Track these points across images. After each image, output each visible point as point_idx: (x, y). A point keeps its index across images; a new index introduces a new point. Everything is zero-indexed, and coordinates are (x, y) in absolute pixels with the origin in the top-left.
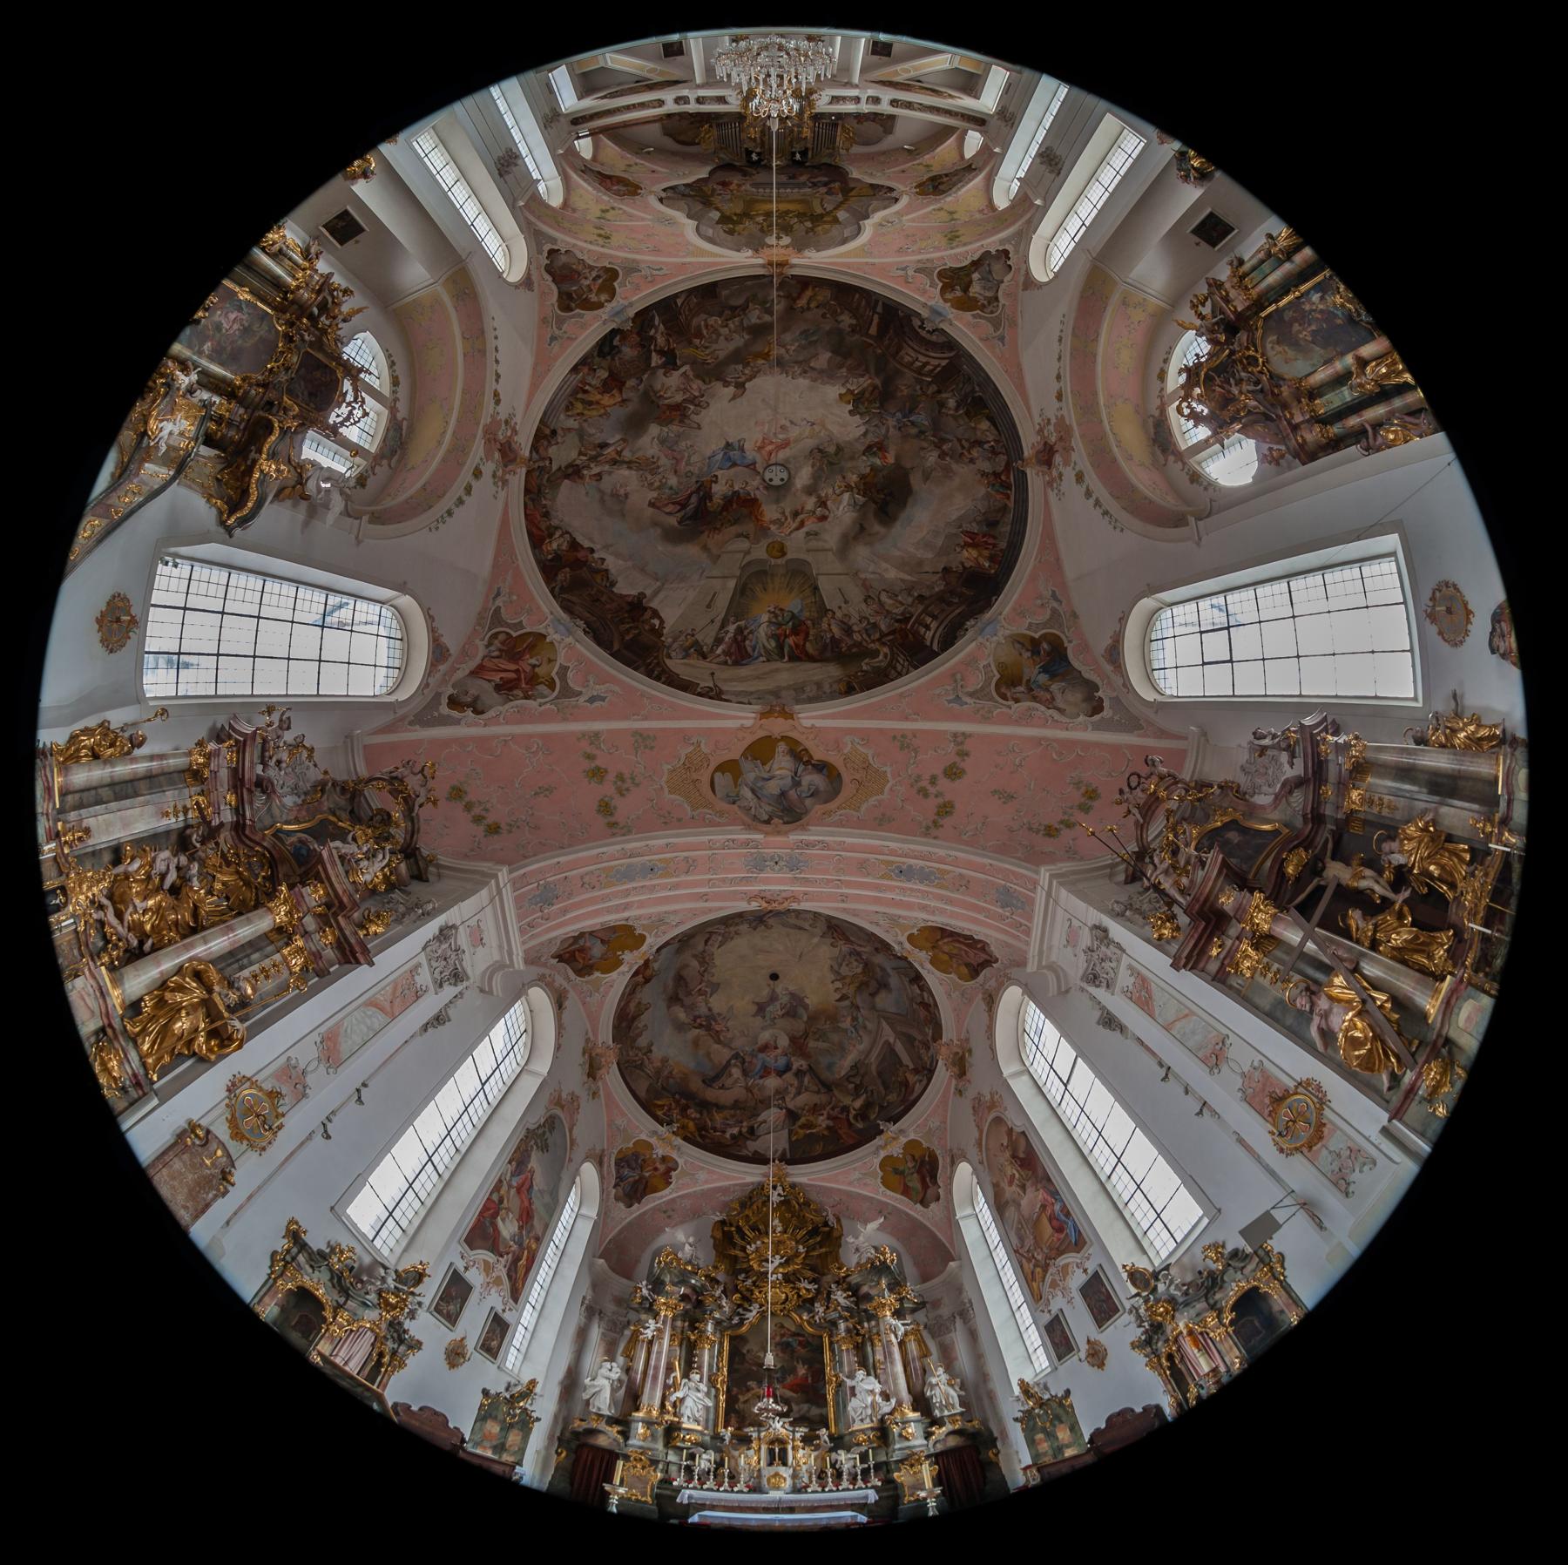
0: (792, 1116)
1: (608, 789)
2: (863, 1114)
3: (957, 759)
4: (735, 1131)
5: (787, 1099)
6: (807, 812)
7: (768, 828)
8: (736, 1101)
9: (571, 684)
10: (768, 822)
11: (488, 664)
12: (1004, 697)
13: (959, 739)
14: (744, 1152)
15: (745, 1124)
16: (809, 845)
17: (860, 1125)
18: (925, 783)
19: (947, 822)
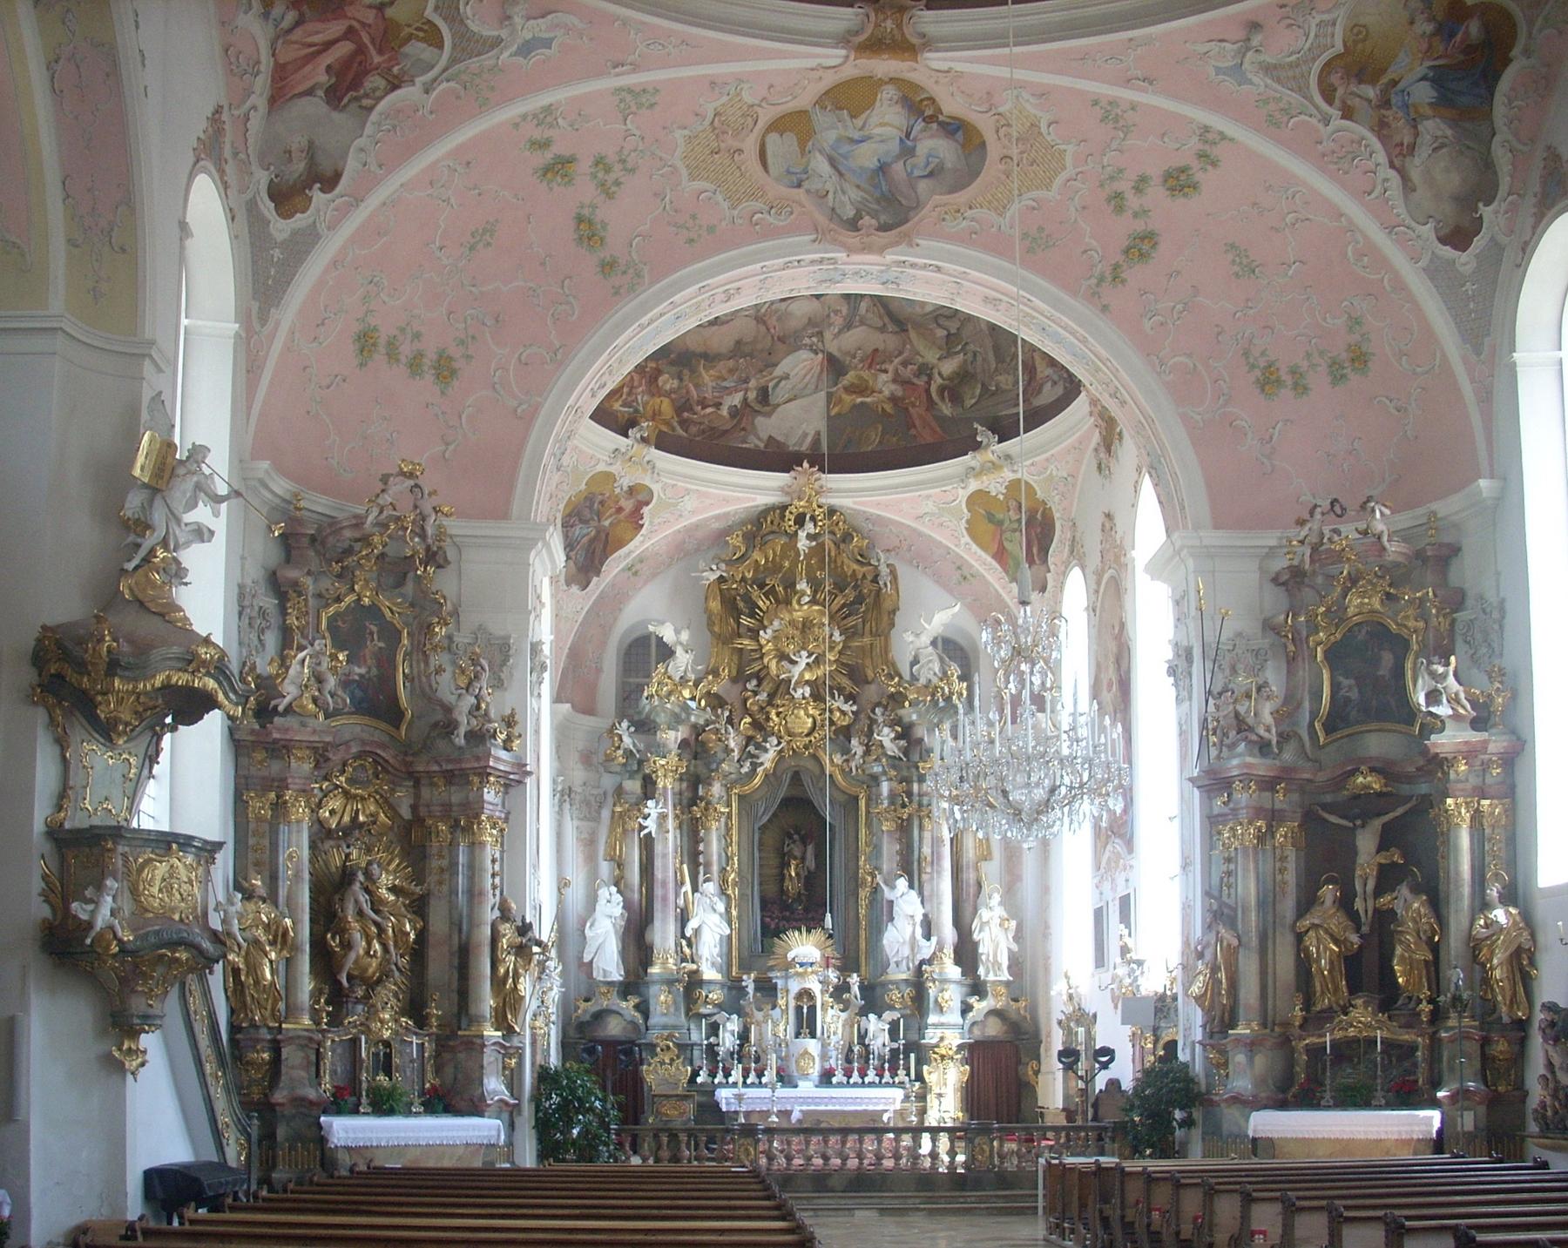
0: (835, 366)
1: (584, 191)
2: (953, 391)
3: (1195, 164)
4: (736, 399)
5: (828, 335)
6: (918, 206)
7: (852, 239)
8: (738, 343)
9: (474, 26)
10: (853, 225)
11: (288, 54)
12: (1328, 94)
13: (1210, 136)
14: (753, 443)
15: (753, 383)
16: (913, 266)
17: (946, 409)
18: (1124, 186)
19: (1136, 275)
